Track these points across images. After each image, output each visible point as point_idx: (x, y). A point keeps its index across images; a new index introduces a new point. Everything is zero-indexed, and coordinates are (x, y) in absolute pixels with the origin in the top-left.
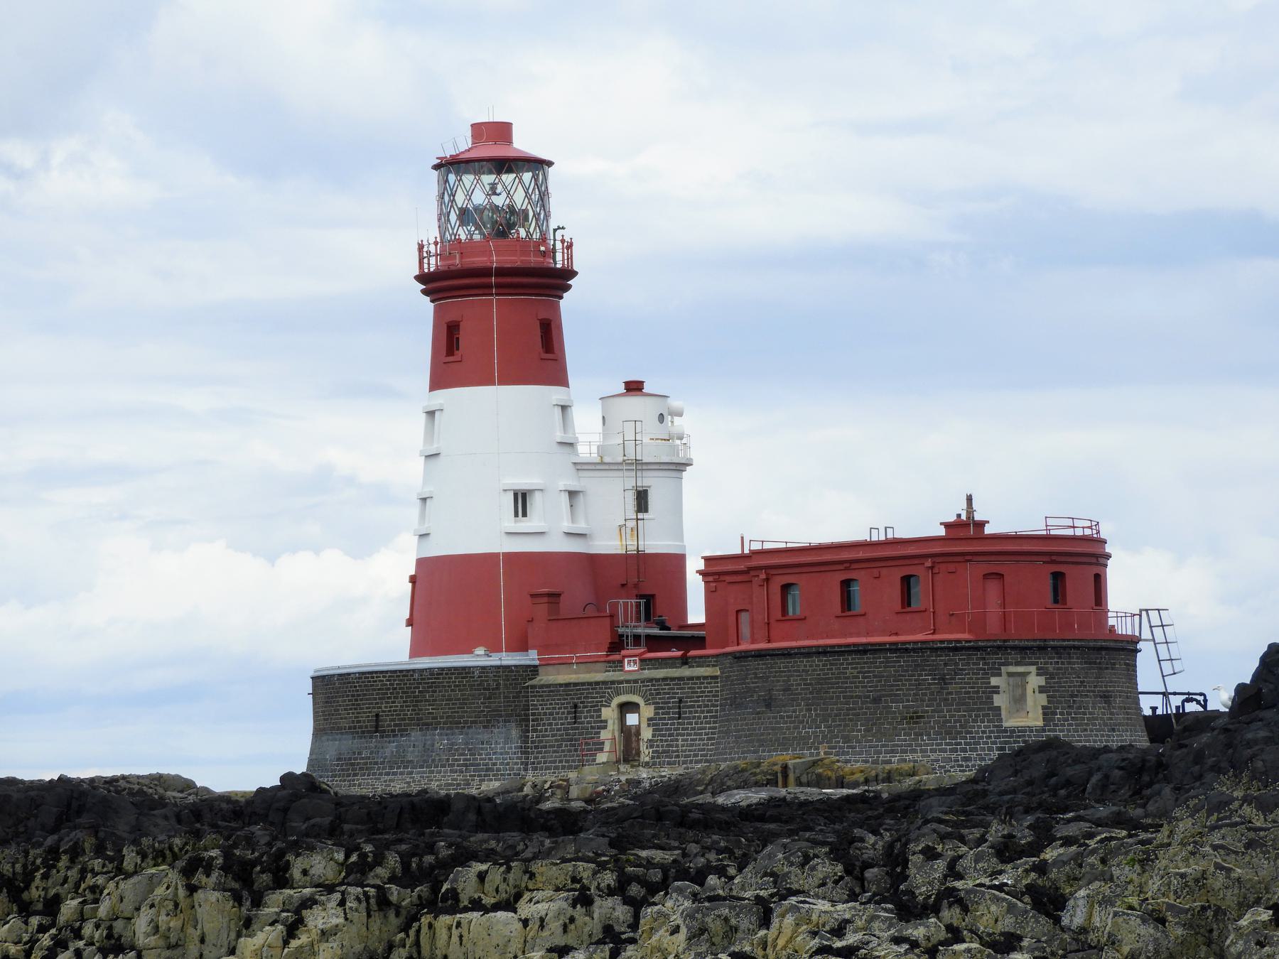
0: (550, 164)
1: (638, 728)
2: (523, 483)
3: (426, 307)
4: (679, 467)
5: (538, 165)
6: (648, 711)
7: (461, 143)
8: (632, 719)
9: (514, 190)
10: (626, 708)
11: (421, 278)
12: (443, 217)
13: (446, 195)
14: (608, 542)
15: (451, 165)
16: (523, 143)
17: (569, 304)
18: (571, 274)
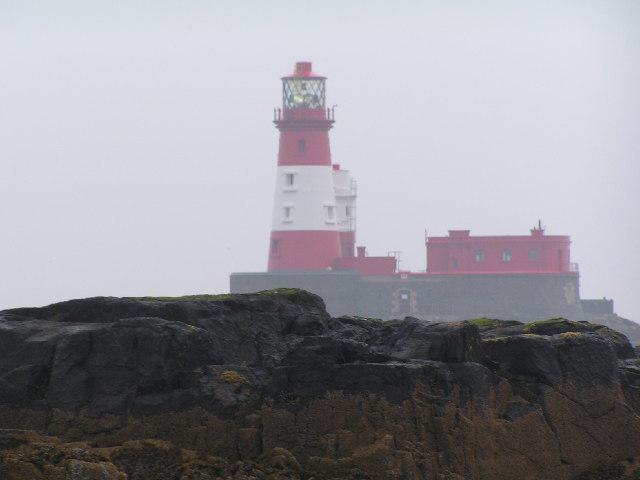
0: (325, 78)
1: (407, 301)
2: (328, 203)
3: (276, 134)
4: (354, 197)
5: (322, 79)
6: (414, 294)
7: (291, 71)
8: (405, 297)
9: (312, 88)
10: (402, 292)
11: (275, 122)
12: (284, 99)
13: (284, 90)
14: (345, 228)
15: (285, 80)
16: (316, 71)
17: (332, 134)
18: (334, 122)
